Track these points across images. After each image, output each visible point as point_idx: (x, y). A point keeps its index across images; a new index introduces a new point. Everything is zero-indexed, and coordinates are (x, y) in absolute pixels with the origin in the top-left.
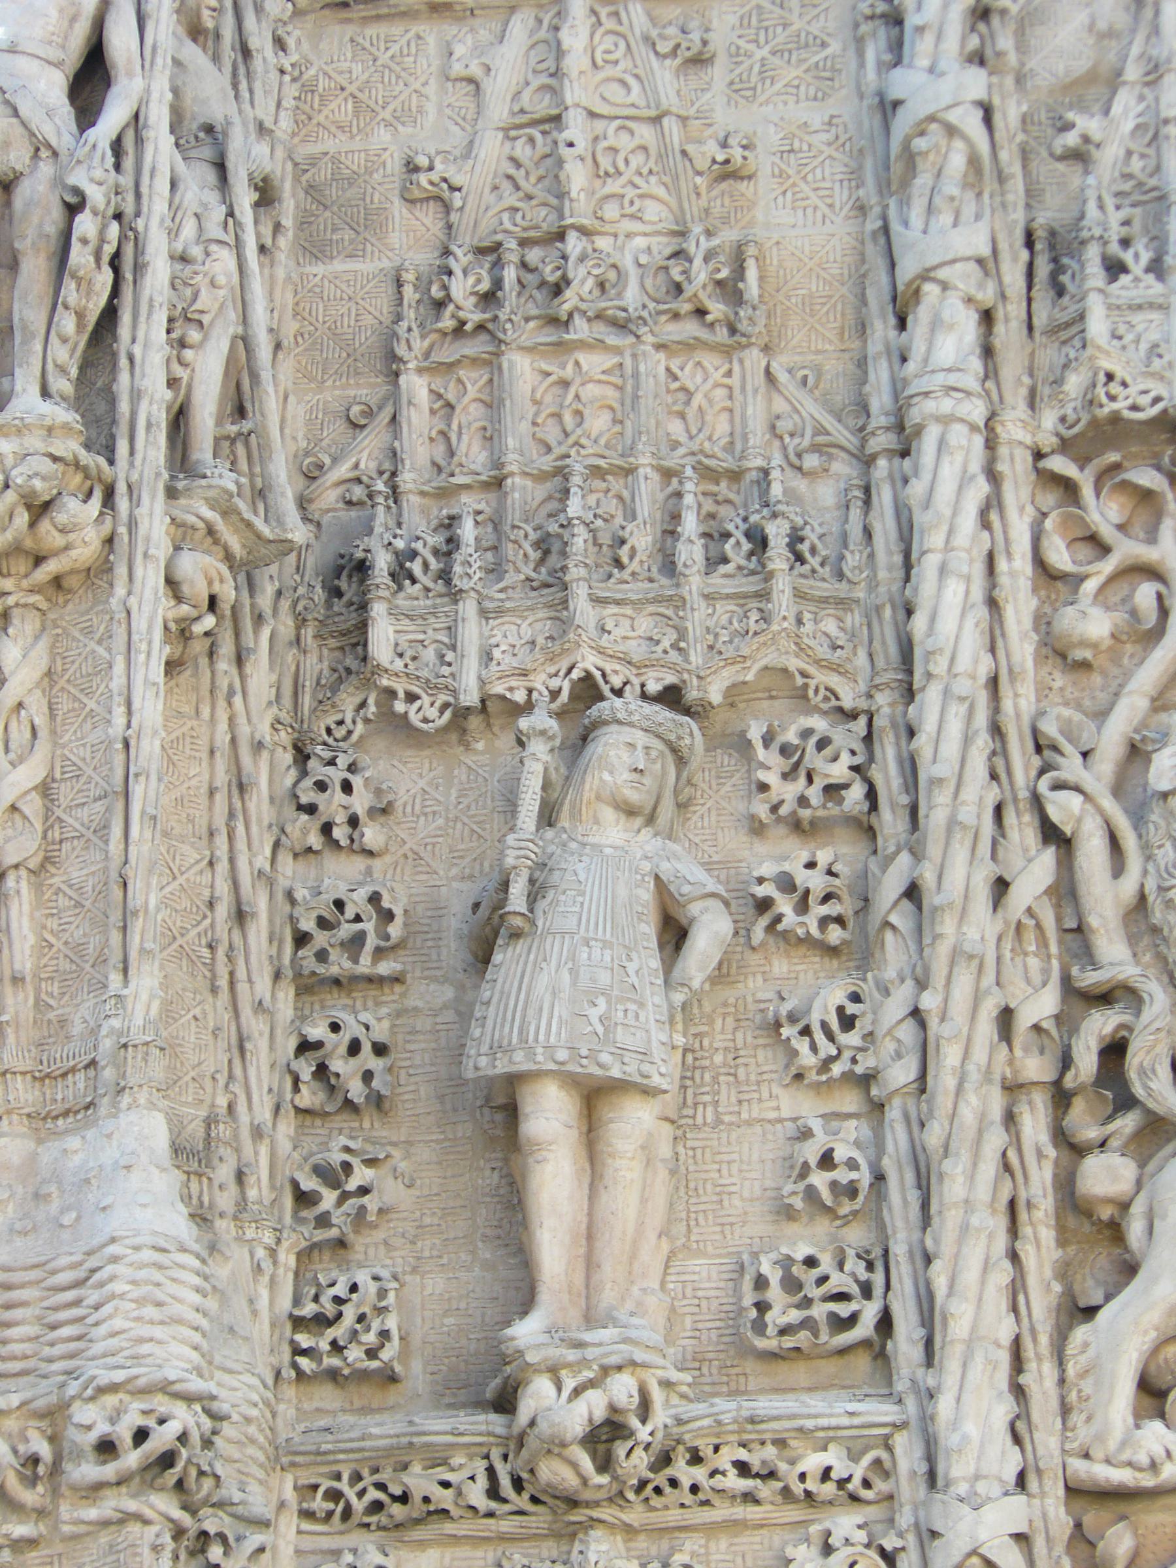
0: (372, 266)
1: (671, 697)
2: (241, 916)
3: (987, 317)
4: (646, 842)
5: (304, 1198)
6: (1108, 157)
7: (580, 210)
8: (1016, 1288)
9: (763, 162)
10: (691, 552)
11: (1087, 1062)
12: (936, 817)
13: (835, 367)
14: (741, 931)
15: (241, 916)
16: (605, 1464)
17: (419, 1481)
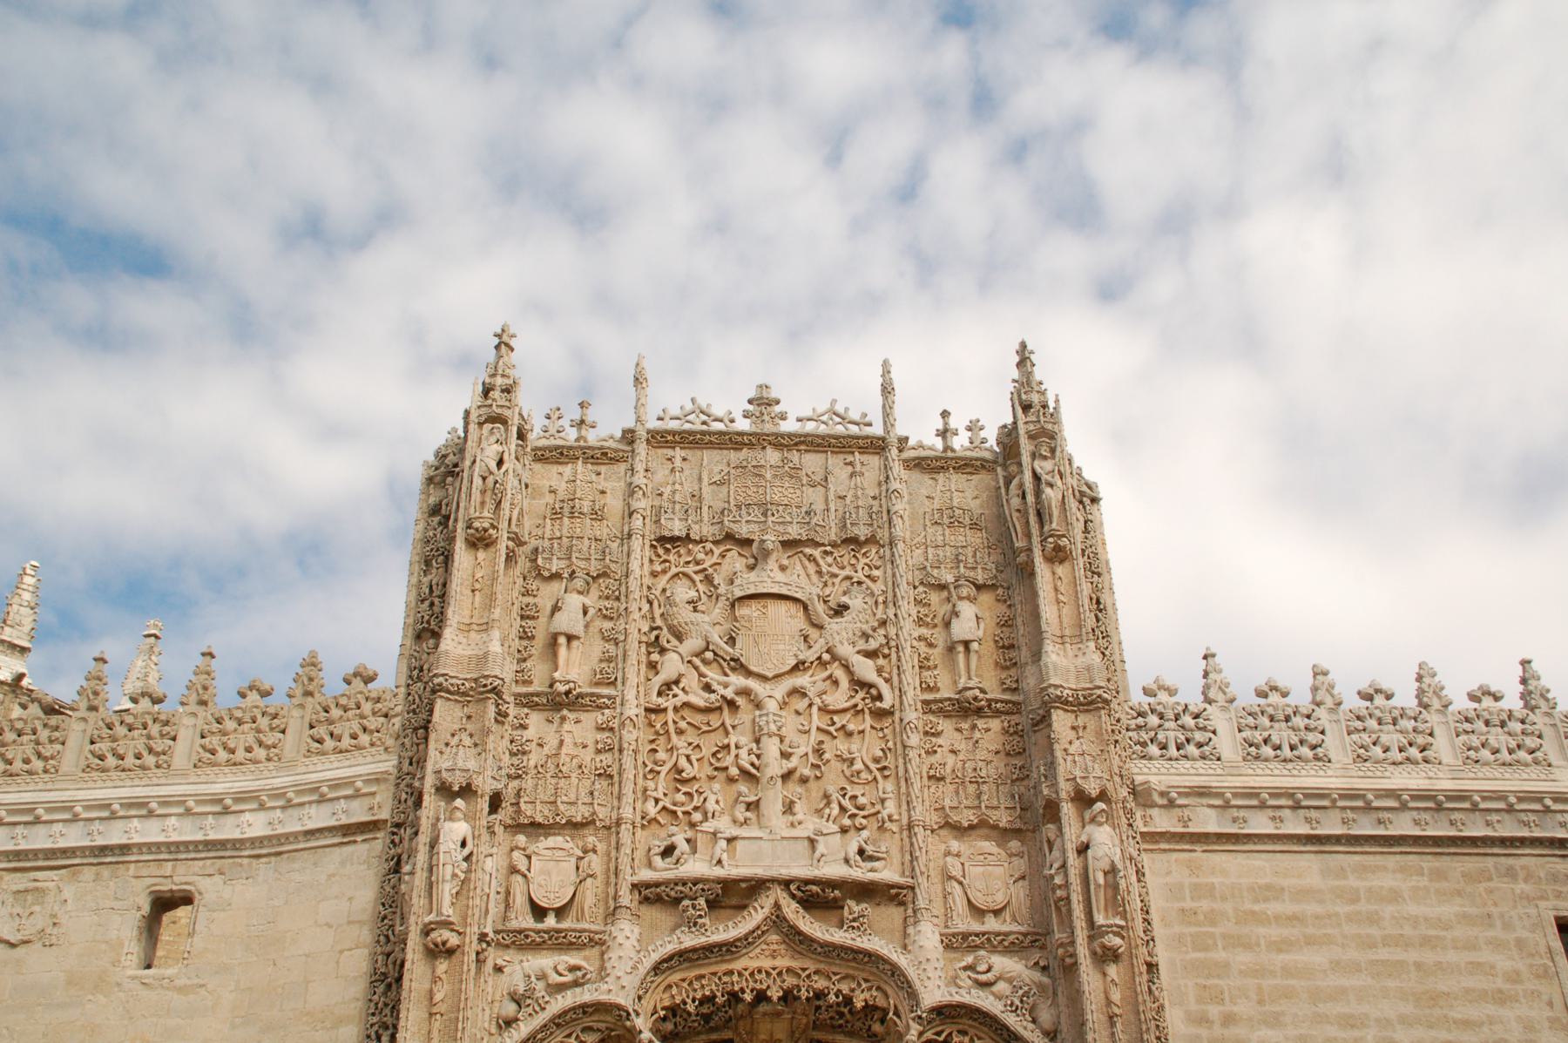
0: (543, 502)
1: (587, 574)
2: (513, 604)
4: (581, 597)
5: (519, 651)
6: (665, 496)
7: (578, 495)
8: (639, 673)
10: (592, 552)
11: (653, 639)
12: (631, 597)
13: (619, 525)
14: (596, 613)
16: (567, 697)
17: (536, 699)
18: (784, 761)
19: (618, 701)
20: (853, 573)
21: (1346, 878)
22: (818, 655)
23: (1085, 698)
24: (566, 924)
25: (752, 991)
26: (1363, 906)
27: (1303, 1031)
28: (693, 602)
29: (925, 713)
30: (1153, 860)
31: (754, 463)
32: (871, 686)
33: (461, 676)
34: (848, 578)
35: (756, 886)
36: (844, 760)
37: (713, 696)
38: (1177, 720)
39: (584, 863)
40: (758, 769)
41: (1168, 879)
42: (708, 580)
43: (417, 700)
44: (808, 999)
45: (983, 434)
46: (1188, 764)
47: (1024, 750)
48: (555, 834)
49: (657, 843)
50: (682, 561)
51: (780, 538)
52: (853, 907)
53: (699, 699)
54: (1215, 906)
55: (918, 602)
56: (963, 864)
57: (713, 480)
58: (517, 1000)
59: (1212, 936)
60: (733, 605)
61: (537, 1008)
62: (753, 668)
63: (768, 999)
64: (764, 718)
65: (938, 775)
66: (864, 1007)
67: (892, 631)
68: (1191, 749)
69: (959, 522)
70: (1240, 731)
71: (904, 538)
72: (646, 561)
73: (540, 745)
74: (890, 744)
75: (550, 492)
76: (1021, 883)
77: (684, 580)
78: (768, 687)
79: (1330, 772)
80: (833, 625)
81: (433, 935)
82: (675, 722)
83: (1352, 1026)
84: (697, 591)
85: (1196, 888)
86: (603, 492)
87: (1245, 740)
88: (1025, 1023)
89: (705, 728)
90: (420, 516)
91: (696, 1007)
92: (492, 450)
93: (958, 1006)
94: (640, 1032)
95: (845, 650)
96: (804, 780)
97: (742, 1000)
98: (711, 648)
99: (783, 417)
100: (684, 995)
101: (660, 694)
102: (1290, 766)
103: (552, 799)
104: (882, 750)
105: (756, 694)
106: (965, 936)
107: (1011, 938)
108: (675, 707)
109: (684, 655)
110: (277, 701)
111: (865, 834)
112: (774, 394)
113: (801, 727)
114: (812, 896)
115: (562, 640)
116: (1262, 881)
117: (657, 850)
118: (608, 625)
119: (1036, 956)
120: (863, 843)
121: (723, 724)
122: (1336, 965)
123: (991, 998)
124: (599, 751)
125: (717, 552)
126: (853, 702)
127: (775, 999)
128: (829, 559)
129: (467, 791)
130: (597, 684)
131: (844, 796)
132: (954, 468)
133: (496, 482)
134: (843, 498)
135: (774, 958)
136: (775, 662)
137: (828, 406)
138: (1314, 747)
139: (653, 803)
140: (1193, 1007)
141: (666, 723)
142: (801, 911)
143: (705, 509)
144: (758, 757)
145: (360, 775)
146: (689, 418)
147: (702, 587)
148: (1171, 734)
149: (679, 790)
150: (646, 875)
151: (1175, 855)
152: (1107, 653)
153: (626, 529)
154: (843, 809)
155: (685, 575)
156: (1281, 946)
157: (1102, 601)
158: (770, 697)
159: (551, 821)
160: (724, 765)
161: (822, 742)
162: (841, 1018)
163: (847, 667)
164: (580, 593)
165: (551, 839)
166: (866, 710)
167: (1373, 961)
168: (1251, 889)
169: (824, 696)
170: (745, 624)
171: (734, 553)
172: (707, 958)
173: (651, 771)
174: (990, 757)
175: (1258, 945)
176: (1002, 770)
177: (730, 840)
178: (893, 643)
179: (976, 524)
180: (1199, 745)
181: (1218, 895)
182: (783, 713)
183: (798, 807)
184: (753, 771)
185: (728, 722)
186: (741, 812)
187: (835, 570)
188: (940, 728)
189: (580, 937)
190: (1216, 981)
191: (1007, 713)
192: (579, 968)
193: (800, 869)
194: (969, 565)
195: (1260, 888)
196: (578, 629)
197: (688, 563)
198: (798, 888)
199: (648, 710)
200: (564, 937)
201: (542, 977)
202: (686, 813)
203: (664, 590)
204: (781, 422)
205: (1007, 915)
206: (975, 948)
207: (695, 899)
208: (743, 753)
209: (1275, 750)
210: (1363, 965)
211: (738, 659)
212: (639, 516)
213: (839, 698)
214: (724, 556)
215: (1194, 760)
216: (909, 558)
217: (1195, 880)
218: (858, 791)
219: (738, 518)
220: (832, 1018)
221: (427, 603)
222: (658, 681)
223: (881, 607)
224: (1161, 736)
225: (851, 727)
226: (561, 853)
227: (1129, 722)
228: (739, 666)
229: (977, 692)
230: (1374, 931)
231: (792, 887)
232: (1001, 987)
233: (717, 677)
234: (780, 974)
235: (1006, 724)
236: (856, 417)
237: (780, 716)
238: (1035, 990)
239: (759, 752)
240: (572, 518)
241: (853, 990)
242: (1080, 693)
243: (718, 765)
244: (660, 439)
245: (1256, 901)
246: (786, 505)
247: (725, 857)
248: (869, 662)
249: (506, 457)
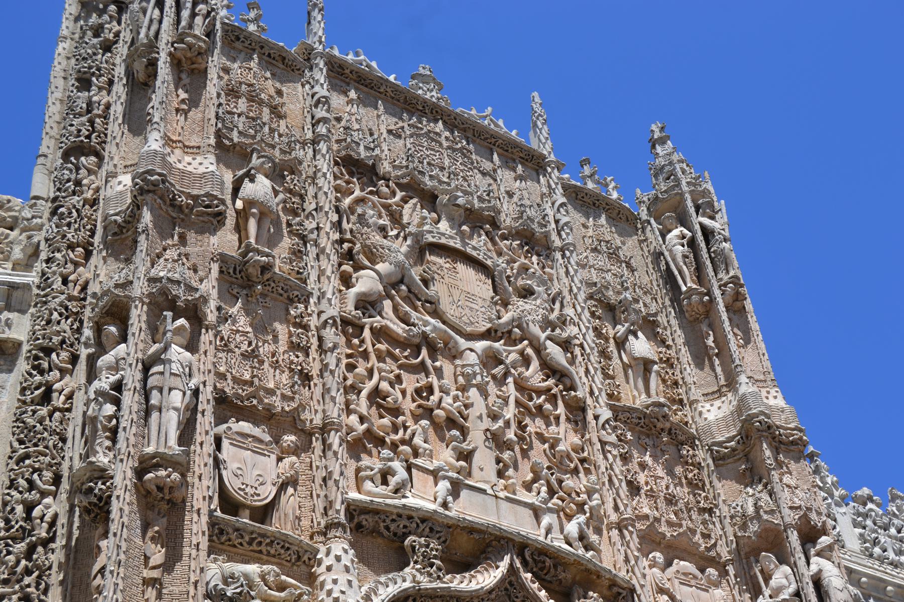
33: (177, 187)
40: (465, 419)
43: (75, 214)
95: (535, 330)
101: (356, 309)
125: (399, 195)
159: (246, 403)
163: (539, 350)
173: (353, 387)
189: (288, 549)
208: (448, 400)
213: (533, 374)
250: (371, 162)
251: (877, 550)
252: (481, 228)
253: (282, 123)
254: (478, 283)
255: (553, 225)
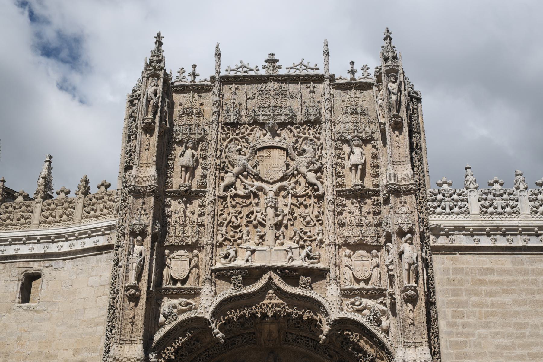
1: (195, 140)
3: (219, 115)
9: (204, 104)
15: (163, 154)
16: (186, 193)
18: (276, 218)
19: (207, 194)
20: (309, 136)
21: (523, 264)
22: (292, 172)
23: (405, 189)
24: (185, 286)
25: (261, 313)
26: (530, 278)
27: (498, 330)
28: (239, 151)
29: (338, 196)
30: (436, 258)
31: (267, 89)
32: (315, 185)
34: (306, 138)
35: (263, 270)
36: (302, 217)
37: (247, 191)
38: (451, 196)
39: (193, 261)
40: (265, 221)
41: (443, 266)
42: (247, 141)
44: (283, 316)
45: (369, 71)
46: (455, 216)
47: (381, 211)
48: (181, 250)
49: (222, 252)
50: (235, 134)
51: (277, 122)
52: (303, 279)
53: (241, 191)
54: (463, 277)
55: (337, 148)
56: (351, 260)
57: (249, 97)
58: (166, 316)
59: (461, 290)
60: (256, 151)
61: (173, 320)
62: (264, 178)
63: (268, 316)
64: (268, 200)
65: (342, 222)
66: (307, 319)
67: (324, 161)
68: (456, 210)
69: (356, 112)
70: (479, 201)
71: (331, 120)
72: (219, 133)
73: (175, 213)
74: (322, 209)
75: (180, 105)
76: (376, 268)
77: (236, 142)
78: (270, 186)
79: (519, 219)
80: (298, 159)
81: (129, 291)
82: (231, 202)
83: (521, 328)
84: (241, 146)
85: (454, 269)
86: (202, 105)
87: (481, 205)
88: (374, 327)
89: (243, 204)
90: (126, 117)
91: (238, 319)
92: (151, 90)
93: (346, 320)
94: (214, 329)
95: (304, 170)
96: (286, 227)
97: (257, 317)
98: (246, 170)
99: (280, 67)
100: (233, 314)
101: (224, 191)
102: (501, 216)
103: (180, 235)
104: (319, 212)
105: (265, 190)
106: (350, 290)
107: (371, 291)
108: (231, 197)
109: (235, 173)
110: (71, 196)
111: (309, 248)
112: (276, 57)
113: (284, 203)
114: (286, 274)
115: (183, 169)
116: (485, 266)
117: (222, 256)
118: (203, 162)
119: (381, 299)
120: (309, 253)
121: (251, 203)
122: (515, 302)
123: (361, 316)
124: (200, 215)
125: (250, 128)
126: (307, 191)
127: (270, 316)
128: (298, 130)
129: (143, 233)
130: (201, 187)
131: (301, 232)
132: (355, 88)
133: (154, 103)
134: (304, 103)
135: (271, 300)
136: (274, 176)
137: (300, 62)
138: (512, 208)
139: (221, 236)
140: (450, 320)
141: (227, 203)
142: (281, 280)
143: (244, 110)
144: (265, 216)
145: (103, 227)
146: (239, 70)
147: (245, 144)
148: (447, 203)
149: (232, 231)
150: (218, 265)
151: (446, 256)
152: (420, 168)
153: (211, 121)
154: (301, 238)
155: (236, 139)
156: (490, 294)
157: (419, 145)
158: (271, 191)
159: (179, 244)
160: (251, 220)
161: (293, 210)
162: (298, 324)
163: (305, 177)
164: (192, 149)
165: (179, 251)
166: (312, 196)
167: (532, 300)
168: (480, 270)
169: (294, 190)
170: (260, 159)
171: (257, 128)
172: (241, 299)
173: (221, 223)
174: (366, 214)
175: (481, 294)
176: (372, 220)
177: (253, 252)
178: (324, 166)
179: (364, 113)
180: (460, 208)
181: (464, 273)
182: (276, 197)
183: (281, 237)
184: (263, 222)
185: (253, 202)
186: (256, 239)
187: (301, 135)
188: (344, 202)
190: (461, 309)
191: (373, 195)
192: (191, 304)
193: (282, 262)
194: (360, 131)
195: (484, 269)
196: (191, 164)
197: (237, 134)
198: (280, 271)
199: (219, 197)
200: (184, 291)
201: (175, 307)
202: (235, 240)
203: (227, 146)
204: (279, 70)
205: (370, 282)
206: (356, 295)
207: (238, 276)
208: (259, 215)
209: (512, 209)
210: (528, 302)
211: (258, 175)
212: (216, 114)
214: (253, 131)
215: (458, 214)
216: (333, 128)
217: (454, 266)
218: (307, 230)
219: (259, 114)
220: (295, 324)
221: (129, 154)
222: (223, 184)
223: (320, 150)
224: (443, 204)
225: (305, 203)
226: (183, 257)
227: (429, 198)
228: (259, 178)
229: (360, 187)
230: (534, 288)
231: (278, 271)
232: (366, 312)
233: (249, 183)
234: (272, 306)
235: (373, 200)
236: (313, 67)
237: (275, 199)
238: (380, 312)
239: (266, 214)
240: (189, 116)
241: (303, 313)
242: (403, 187)
243: (248, 220)
244: (226, 80)
245: (481, 275)
246: (280, 107)
247: (250, 258)
248: (314, 175)
249: (158, 91)
250: (236, 121)
251: (491, 210)
252: (286, 128)
253: (202, 118)
254: (280, 157)
255: (323, 111)
